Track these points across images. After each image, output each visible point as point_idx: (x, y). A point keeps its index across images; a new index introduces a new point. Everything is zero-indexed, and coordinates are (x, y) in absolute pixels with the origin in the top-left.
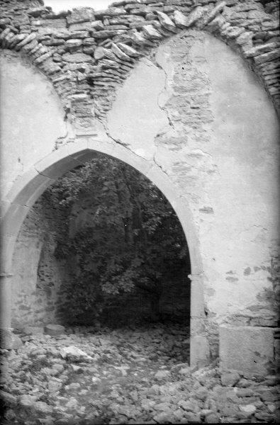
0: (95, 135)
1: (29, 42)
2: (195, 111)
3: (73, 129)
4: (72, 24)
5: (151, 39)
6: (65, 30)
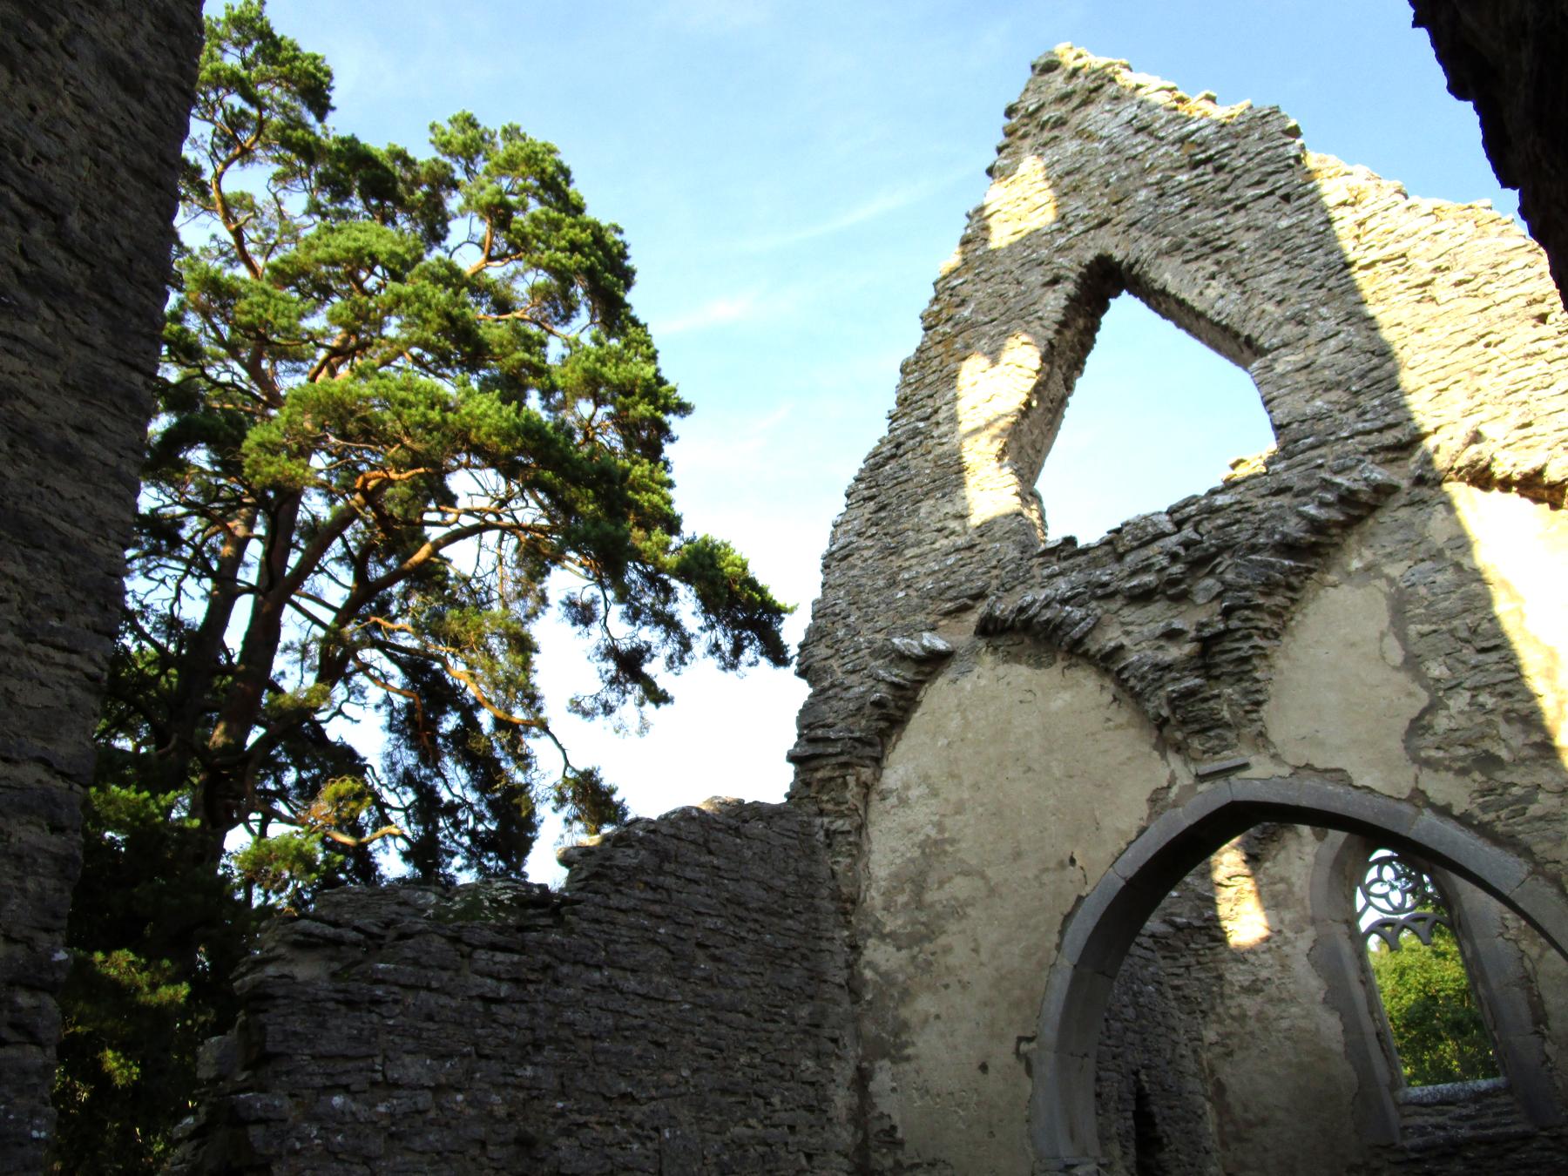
0: (1245, 766)
1: (1047, 605)
2: (1494, 656)
3: (1186, 764)
4: (1127, 552)
5: (1316, 526)
6: (1116, 567)
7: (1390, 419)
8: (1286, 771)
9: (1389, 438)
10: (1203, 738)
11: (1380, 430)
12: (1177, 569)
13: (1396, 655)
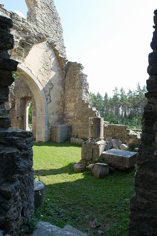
7: (47, 31)
8: (25, 67)
9: (46, 34)
10: (18, 56)
11: (46, 32)
12: (22, 29)
13: (40, 61)
